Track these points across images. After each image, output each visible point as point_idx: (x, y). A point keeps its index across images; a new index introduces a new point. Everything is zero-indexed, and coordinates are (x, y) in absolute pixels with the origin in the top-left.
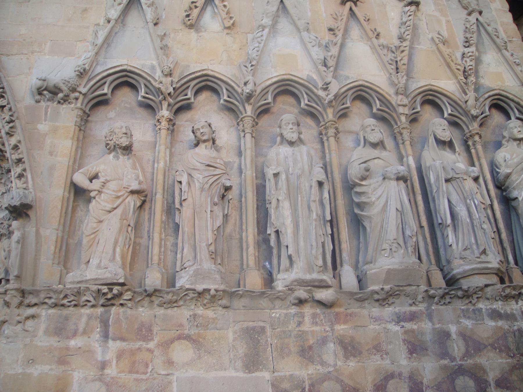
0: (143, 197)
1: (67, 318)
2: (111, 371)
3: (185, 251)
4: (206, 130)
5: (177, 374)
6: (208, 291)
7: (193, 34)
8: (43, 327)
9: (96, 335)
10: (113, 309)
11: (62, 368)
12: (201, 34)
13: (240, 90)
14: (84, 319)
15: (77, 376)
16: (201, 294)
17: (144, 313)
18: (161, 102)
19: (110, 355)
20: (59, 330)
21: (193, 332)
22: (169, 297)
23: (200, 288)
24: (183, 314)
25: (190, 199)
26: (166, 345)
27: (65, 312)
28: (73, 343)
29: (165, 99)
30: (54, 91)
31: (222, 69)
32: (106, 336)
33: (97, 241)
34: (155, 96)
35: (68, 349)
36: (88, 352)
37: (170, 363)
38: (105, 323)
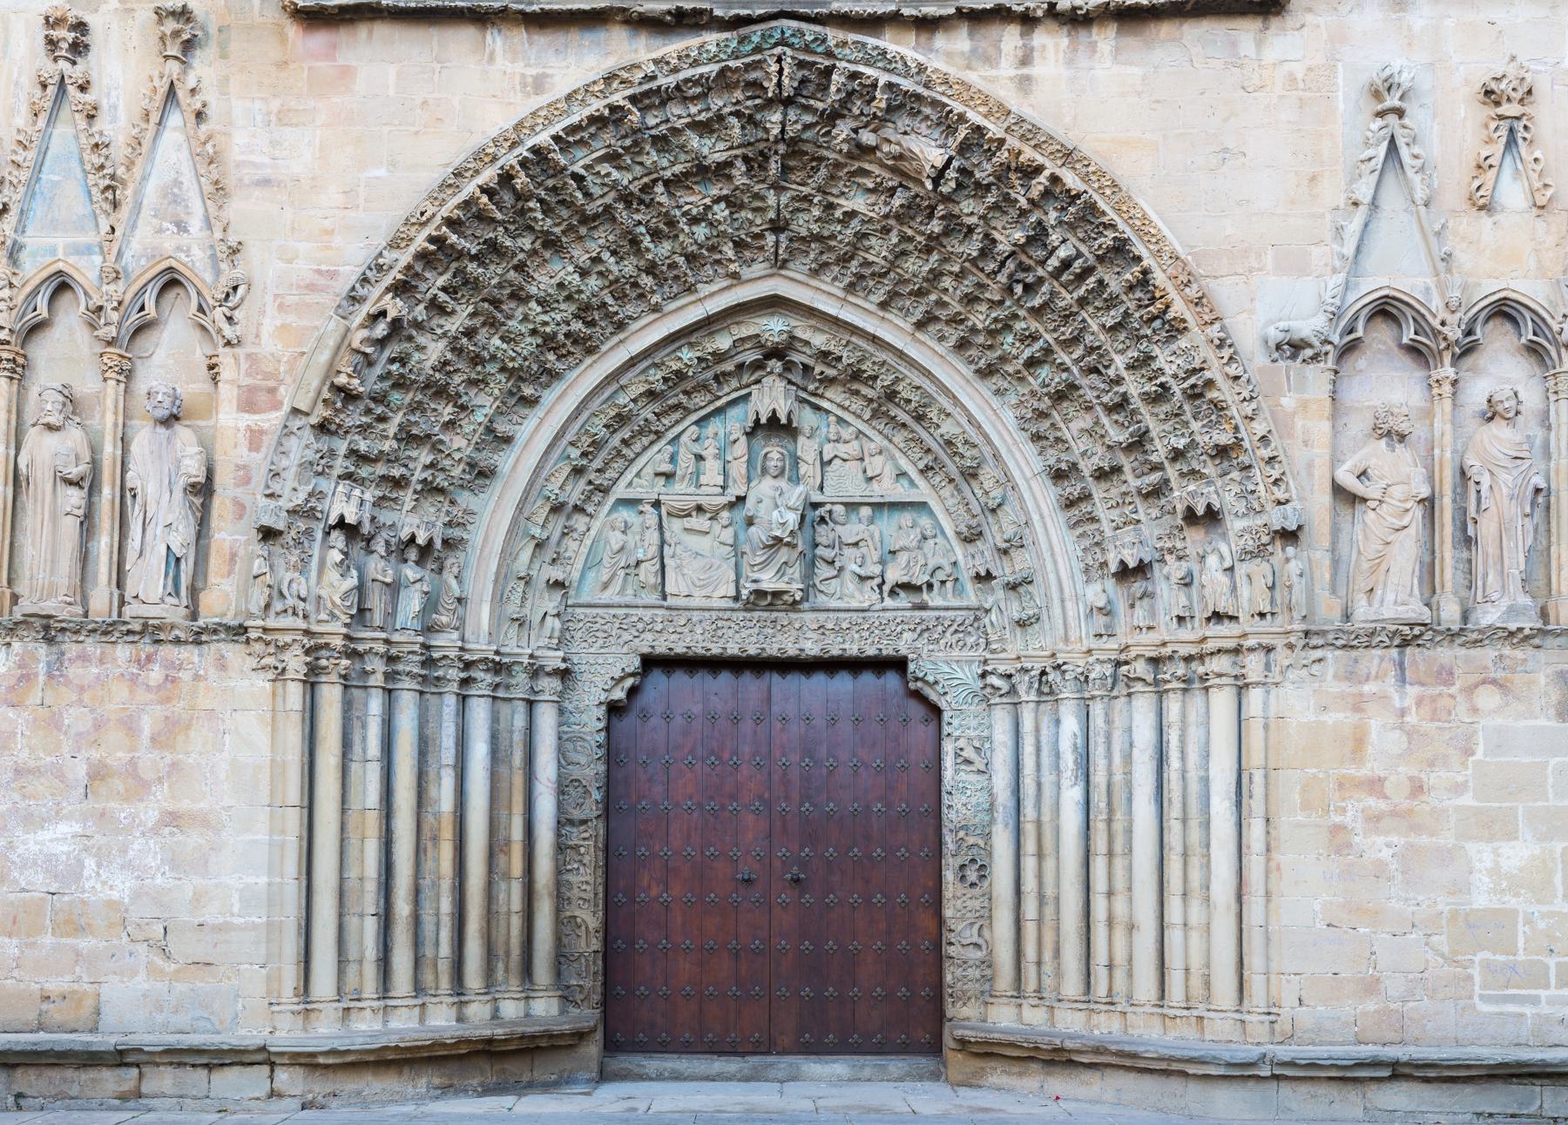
0: (1429, 504)
1: (1356, 661)
2: (1411, 719)
3: (1490, 577)
4: (1513, 403)
5: (1483, 722)
6: (1520, 630)
7: (1485, 220)
8: (1331, 672)
9: (1391, 679)
10: (1408, 650)
11: (1357, 716)
12: (1497, 217)
13: (1556, 328)
14: (1376, 661)
15: (1374, 725)
16: (1512, 634)
17: (1445, 654)
18: (1440, 352)
19: (1409, 701)
20: (1350, 676)
21: (1500, 675)
22: (1475, 636)
23: (1513, 627)
24: (1488, 654)
25: (1493, 508)
26: (1470, 690)
27: (1354, 653)
28: (1366, 688)
29: (1447, 348)
30: (1294, 347)
31: (1530, 289)
32: (1402, 680)
33: (1384, 567)
34: (1427, 336)
35: (1361, 695)
36: (1384, 698)
37: (1475, 710)
38: (1401, 666)
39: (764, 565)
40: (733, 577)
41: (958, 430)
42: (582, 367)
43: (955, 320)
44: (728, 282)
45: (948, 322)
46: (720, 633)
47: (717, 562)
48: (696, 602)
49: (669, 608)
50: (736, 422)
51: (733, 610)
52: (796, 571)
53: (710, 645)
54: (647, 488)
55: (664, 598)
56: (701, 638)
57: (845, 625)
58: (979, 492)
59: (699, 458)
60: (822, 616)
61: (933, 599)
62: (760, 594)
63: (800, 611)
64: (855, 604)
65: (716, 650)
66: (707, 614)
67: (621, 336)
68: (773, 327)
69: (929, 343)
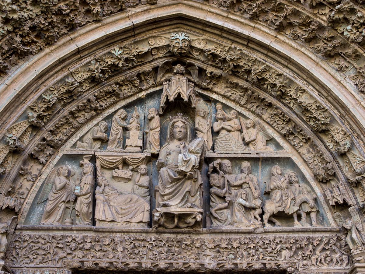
39: (173, 195)
40: (148, 207)
41: (312, 101)
42: (42, 54)
43: (306, 24)
44: (149, 7)
45: (301, 25)
46: (136, 251)
47: (135, 197)
48: (119, 226)
49: (97, 231)
50: (152, 107)
51: (147, 232)
52: (197, 200)
53: (128, 261)
54: (86, 148)
55: (94, 224)
56: (121, 255)
57: (235, 245)
58: (330, 145)
59: (125, 129)
60: (217, 237)
61: (297, 225)
62: (169, 216)
63: (200, 233)
64: (242, 228)
65: (133, 264)
66: (126, 236)
67: (72, 36)
68: (179, 38)
69: (287, 41)
